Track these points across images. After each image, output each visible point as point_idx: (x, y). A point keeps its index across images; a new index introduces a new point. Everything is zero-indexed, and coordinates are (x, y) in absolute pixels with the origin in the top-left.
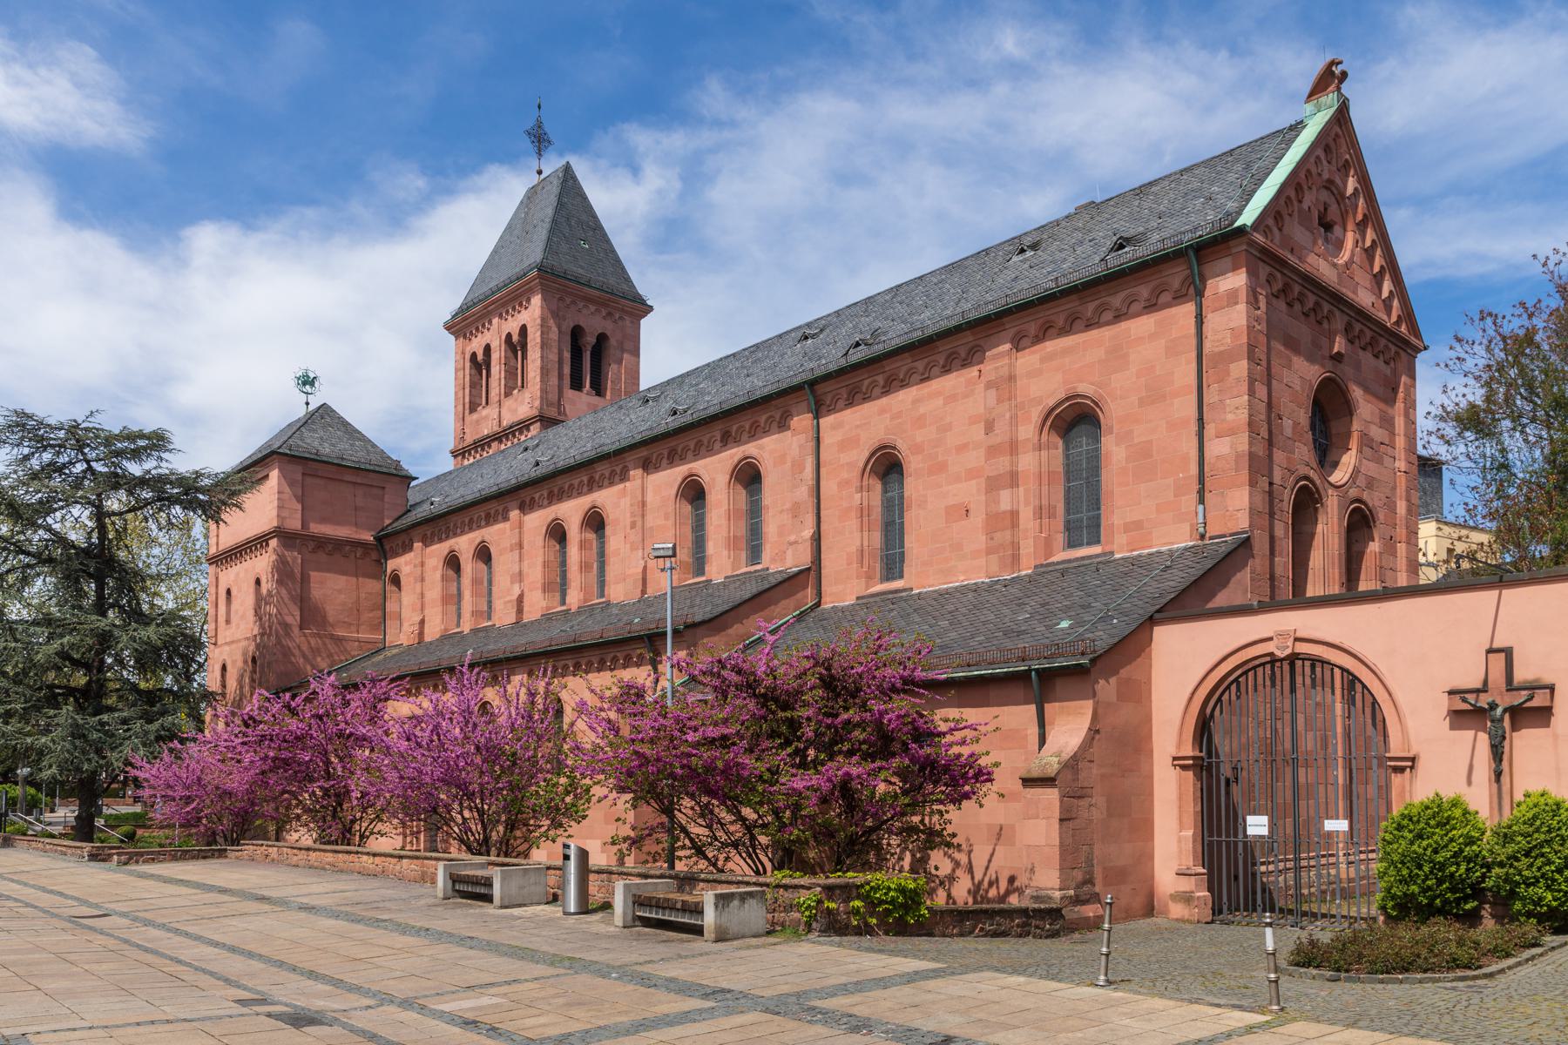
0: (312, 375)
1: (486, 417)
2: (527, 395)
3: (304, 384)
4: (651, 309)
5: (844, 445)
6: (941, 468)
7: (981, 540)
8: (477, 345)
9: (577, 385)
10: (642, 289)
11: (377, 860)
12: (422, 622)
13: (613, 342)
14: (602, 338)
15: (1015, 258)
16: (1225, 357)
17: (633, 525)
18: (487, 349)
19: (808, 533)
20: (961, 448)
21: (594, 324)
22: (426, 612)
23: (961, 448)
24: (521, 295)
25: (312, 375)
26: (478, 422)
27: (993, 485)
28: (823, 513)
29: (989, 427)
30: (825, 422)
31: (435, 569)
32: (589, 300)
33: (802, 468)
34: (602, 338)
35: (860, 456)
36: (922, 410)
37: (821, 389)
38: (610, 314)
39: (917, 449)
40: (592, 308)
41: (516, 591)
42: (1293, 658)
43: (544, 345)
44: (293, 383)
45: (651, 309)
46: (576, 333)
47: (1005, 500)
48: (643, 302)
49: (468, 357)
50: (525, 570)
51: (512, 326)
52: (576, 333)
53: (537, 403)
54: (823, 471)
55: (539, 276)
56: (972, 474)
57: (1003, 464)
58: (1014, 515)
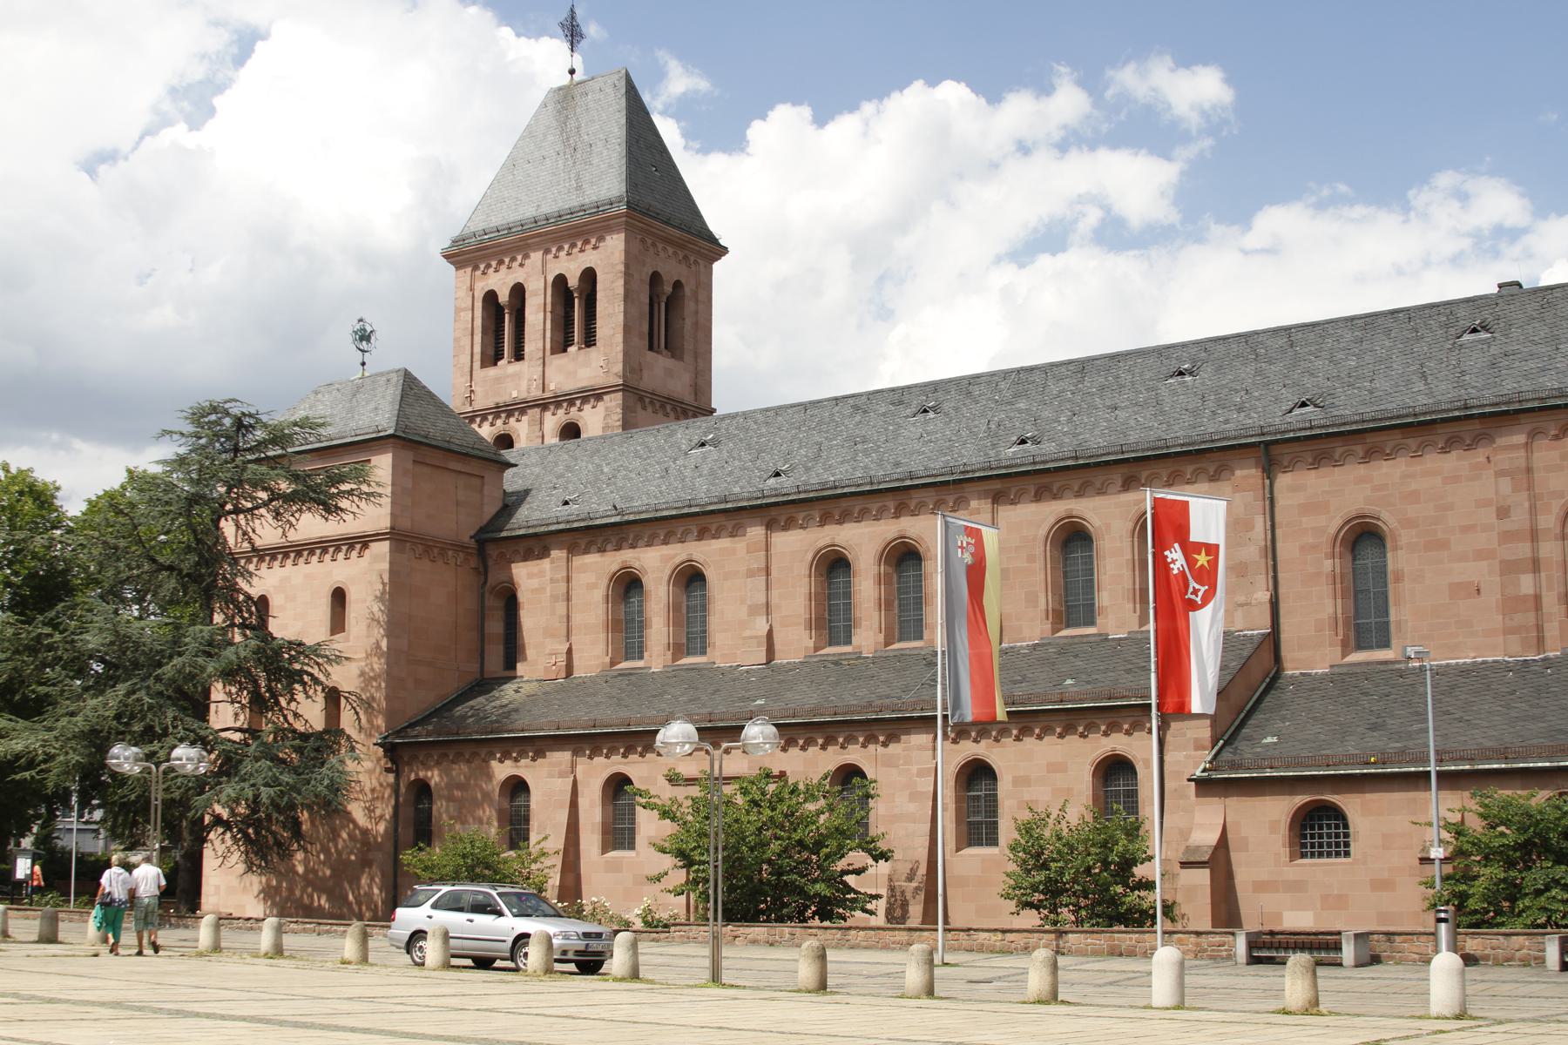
0: (369, 329)
1: (517, 376)
2: (595, 356)
3: (362, 338)
4: (724, 251)
5: (1309, 508)
6: (1443, 545)
8: (500, 282)
9: (651, 348)
11: (1010, 937)
12: (569, 652)
13: (688, 290)
14: (678, 285)
15: (1467, 337)
18: (518, 291)
19: (1264, 596)
20: (1466, 529)
21: (672, 271)
22: (574, 639)
23: (1466, 529)
24: (590, 232)
25: (369, 329)
26: (498, 380)
27: (1509, 568)
28: (1280, 575)
29: (1503, 513)
30: (1283, 481)
31: (591, 587)
32: (667, 241)
33: (1249, 526)
34: (678, 285)
36: (1414, 486)
37: (1275, 450)
38: (686, 257)
39: (1409, 523)
40: (670, 250)
41: (761, 626)
43: (627, 297)
44: (350, 339)
45: (724, 251)
46: (655, 278)
47: (1526, 584)
48: (712, 239)
49: (479, 295)
50: (774, 601)
51: (571, 266)
52: (655, 278)
53: (619, 368)
54: (1278, 532)
55: (627, 215)
56: (1480, 555)
57: (1523, 550)
58: (1537, 598)
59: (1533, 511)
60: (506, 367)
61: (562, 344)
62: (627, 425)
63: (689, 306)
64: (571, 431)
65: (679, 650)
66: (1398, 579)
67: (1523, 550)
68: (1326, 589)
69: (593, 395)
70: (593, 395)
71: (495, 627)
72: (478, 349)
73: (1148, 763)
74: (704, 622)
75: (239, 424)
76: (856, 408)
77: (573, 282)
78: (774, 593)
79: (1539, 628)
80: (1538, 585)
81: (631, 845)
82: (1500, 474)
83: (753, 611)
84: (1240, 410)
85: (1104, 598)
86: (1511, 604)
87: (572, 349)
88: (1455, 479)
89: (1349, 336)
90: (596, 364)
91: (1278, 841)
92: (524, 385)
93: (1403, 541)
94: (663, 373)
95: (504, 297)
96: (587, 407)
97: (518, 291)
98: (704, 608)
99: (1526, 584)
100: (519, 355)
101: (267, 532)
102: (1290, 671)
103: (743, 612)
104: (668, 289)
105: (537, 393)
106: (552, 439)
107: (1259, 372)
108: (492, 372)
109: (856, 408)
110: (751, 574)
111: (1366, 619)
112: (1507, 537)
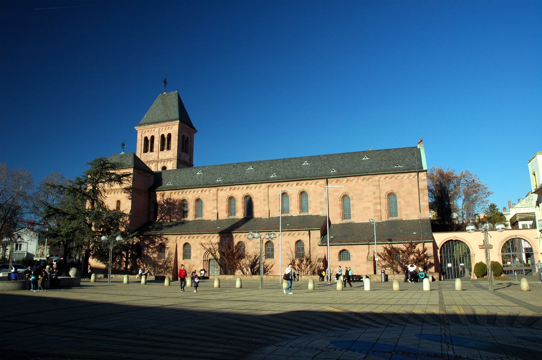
1: (152, 155)
6: (362, 199)
7: (373, 214)
9: (183, 151)
10: (194, 126)
14: (187, 138)
16: (423, 189)
17: (264, 200)
18: (153, 137)
20: (367, 196)
21: (187, 135)
23: (367, 196)
26: (147, 156)
27: (375, 204)
29: (374, 193)
35: (340, 194)
41: (216, 211)
42: (456, 241)
46: (183, 136)
47: (379, 207)
50: (218, 206)
52: (183, 136)
56: (369, 201)
57: (378, 201)
58: (381, 210)
59: (380, 193)
60: (149, 153)
61: (162, 149)
62: (178, 167)
63: (189, 142)
64: (164, 168)
65: (196, 216)
66: (353, 205)
67: (378, 201)
68: (338, 207)
69: (169, 160)
70: (169, 160)
71: (152, 210)
72: (143, 149)
73: (307, 241)
74: (202, 210)
75: (104, 163)
76: (234, 166)
77: (166, 136)
78: (219, 205)
79: (381, 216)
80: (381, 207)
81: (190, 258)
82: (374, 186)
83: (214, 208)
84: (320, 170)
85: (291, 208)
86: (376, 211)
87: (165, 150)
88: (365, 186)
89: (340, 157)
90: (173, 153)
91: (336, 258)
92: (153, 157)
93: (354, 198)
94: (185, 156)
95: (149, 138)
96: (168, 162)
97: (153, 137)
98: (202, 207)
99: (379, 207)
100: (152, 150)
101: (106, 186)
102: (332, 223)
103: (211, 209)
104: (186, 139)
105: (156, 159)
106: (160, 170)
107: (322, 163)
108: (146, 154)
109: (234, 166)
110: (213, 200)
111: (346, 212)
112: (375, 198)
